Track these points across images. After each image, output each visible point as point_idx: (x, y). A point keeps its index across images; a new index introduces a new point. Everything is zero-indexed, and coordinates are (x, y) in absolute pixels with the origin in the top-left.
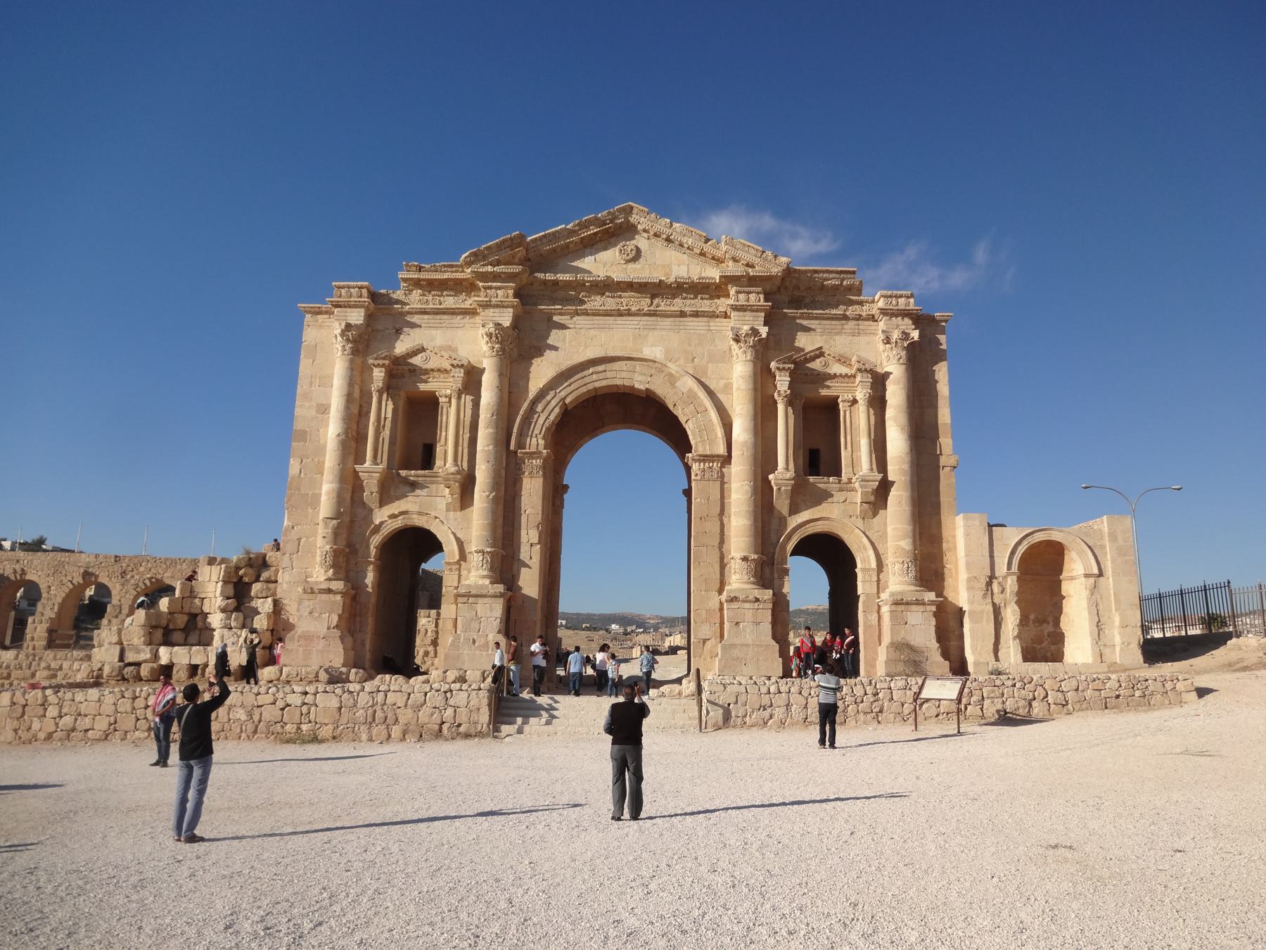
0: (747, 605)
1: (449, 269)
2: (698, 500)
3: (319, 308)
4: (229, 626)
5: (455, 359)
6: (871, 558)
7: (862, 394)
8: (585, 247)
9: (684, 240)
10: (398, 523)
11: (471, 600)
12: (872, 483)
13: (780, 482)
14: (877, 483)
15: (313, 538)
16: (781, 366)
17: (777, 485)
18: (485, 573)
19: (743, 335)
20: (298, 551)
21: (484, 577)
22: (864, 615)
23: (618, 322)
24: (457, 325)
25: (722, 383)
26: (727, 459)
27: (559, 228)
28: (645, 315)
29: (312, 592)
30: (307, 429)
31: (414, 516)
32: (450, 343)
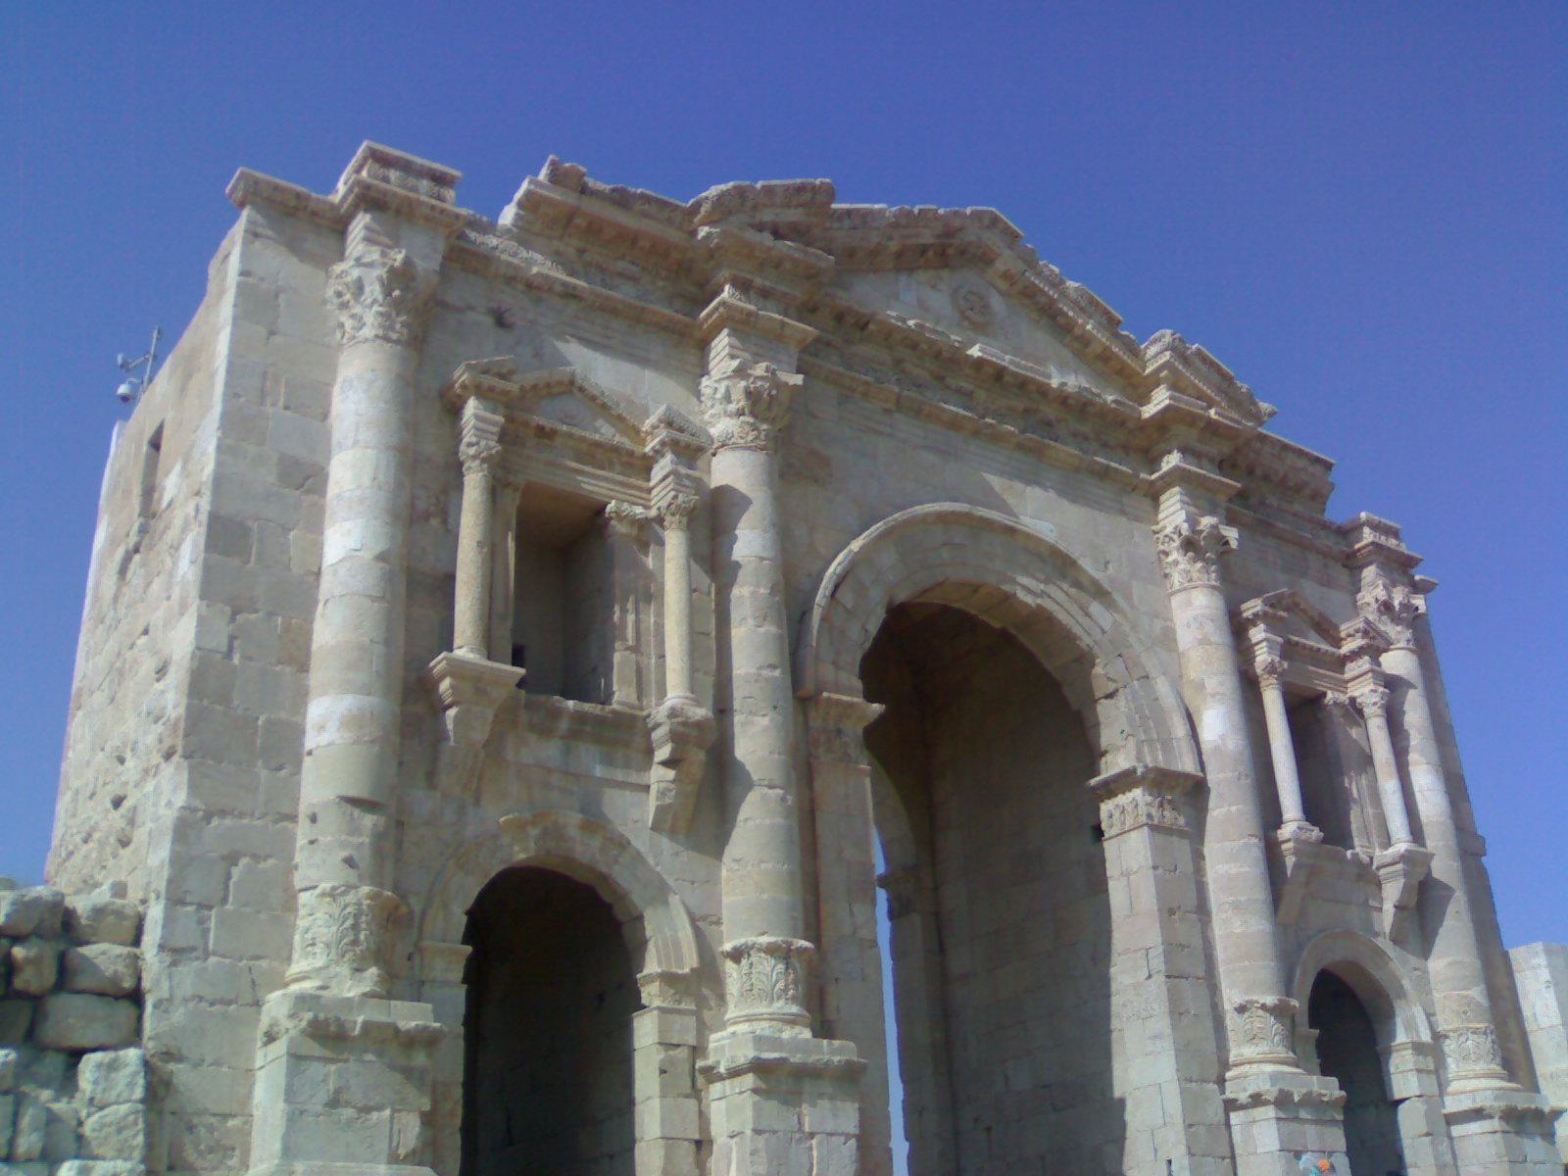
2: (1160, 871)
3: (298, 196)
5: (681, 430)
6: (1418, 1021)
7: (1367, 692)
8: (898, 269)
15: (271, 862)
17: (1296, 852)
18: (794, 1009)
19: (1204, 534)
20: (225, 900)
21: (792, 1021)
22: (1432, 1142)
25: (1158, 625)
27: (877, 206)
30: (249, 523)
32: (629, 391)
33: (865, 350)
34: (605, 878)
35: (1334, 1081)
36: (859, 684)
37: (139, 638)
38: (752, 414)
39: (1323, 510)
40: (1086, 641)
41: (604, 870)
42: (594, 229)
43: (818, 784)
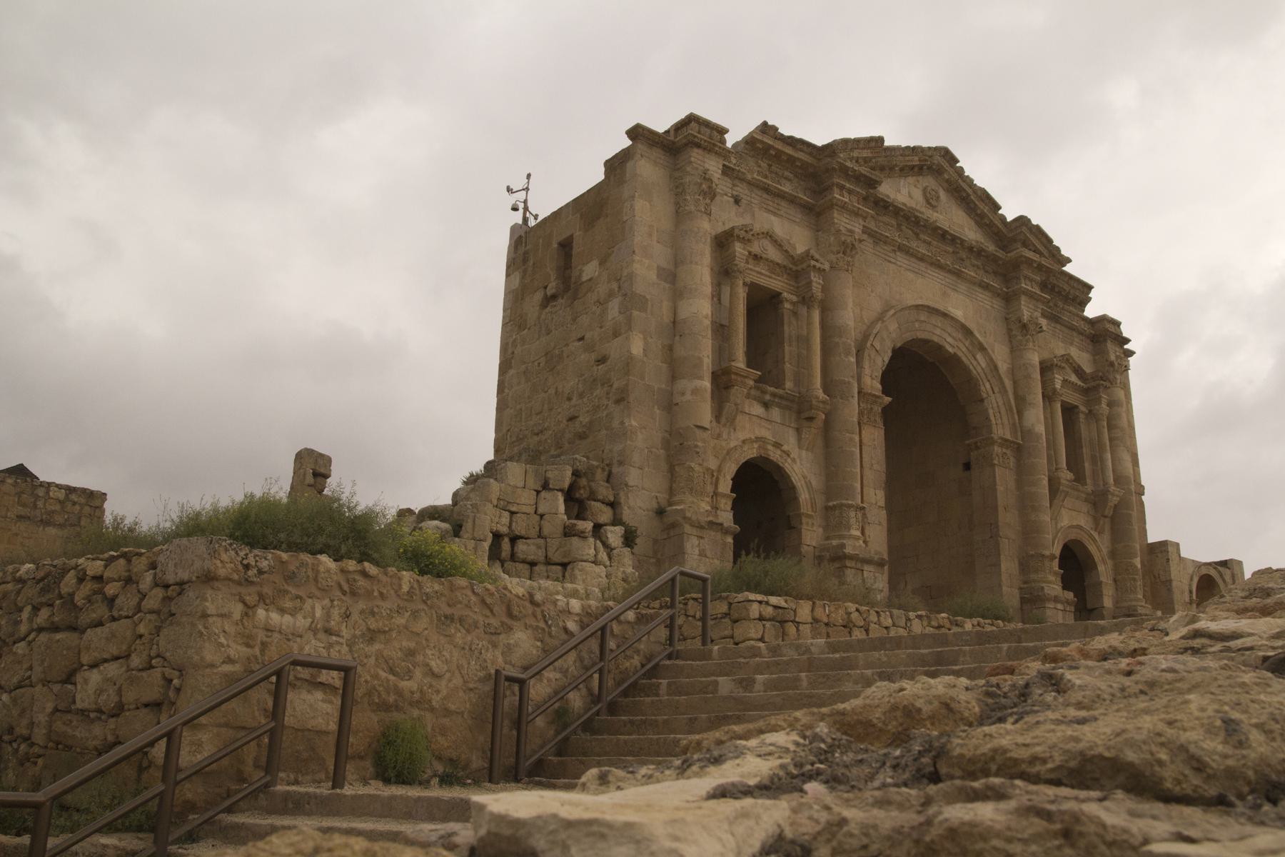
0: (1060, 606)
1: (805, 148)
4: (593, 559)
5: (817, 261)
9: (981, 205)
10: (751, 453)
11: (859, 565)
12: (1115, 498)
13: (1064, 482)
14: (1118, 499)
16: (1059, 364)
23: (929, 271)
24: (794, 219)
26: (1019, 450)
28: (950, 271)
29: (702, 527)
30: (648, 297)
31: (770, 447)
33: (886, 219)
34: (780, 469)
35: (1070, 595)
36: (879, 386)
37: (573, 341)
38: (844, 253)
39: (1084, 311)
40: (975, 372)
41: (781, 465)
42: (779, 154)
43: (863, 432)
